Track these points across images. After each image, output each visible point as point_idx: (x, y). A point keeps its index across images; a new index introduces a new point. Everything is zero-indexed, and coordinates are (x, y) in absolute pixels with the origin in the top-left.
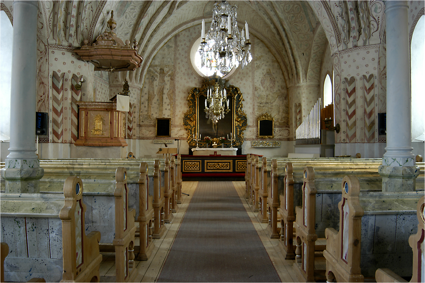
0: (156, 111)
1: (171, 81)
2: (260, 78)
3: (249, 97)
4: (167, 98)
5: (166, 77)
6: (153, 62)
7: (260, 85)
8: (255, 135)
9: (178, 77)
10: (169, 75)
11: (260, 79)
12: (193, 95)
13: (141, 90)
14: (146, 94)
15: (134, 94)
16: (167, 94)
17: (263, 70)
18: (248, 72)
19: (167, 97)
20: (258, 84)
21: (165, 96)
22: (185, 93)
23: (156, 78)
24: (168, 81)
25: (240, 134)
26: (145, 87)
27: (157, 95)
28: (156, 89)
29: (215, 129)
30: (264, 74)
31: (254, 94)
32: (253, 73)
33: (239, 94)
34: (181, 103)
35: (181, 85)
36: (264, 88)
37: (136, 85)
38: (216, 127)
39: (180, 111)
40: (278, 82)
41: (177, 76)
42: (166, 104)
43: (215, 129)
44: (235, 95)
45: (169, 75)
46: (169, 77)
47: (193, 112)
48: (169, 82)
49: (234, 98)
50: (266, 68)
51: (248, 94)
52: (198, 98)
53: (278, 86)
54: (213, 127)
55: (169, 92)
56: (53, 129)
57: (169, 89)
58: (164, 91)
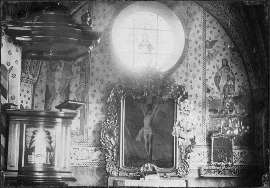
1: (82, 72)
2: (213, 73)
3: (198, 103)
5: (75, 66)
7: (213, 84)
8: (206, 160)
11: (213, 76)
12: (117, 97)
13: (35, 85)
14: (42, 91)
15: (28, 92)
16: (76, 92)
17: (218, 61)
18: (197, 63)
20: (210, 83)
22: (102, 92)
23: (58, 67)
24: (78, 72)
25: (186, 157)
26: (41, 81)
27: (59, 94)
28: (58, 85)
29: (148, 149)
30: (219, 68)
31: (204, 97)
32: (204, 65)
33: (184, 96)
34: (96, 108)
35: (97, 80)
36: (219, 89)
38: (150, 146)
40: (238, 80)
43: (148, 149)
44: (179, 97)
45: (79, 64)
46: (79, 67)
47: (115, 122)
48: (79, 75)
49: (177, 102)
50: (222, 57)
51: (196, 96)
52: (123, 100)
53: (239, 86)
54: (146, 146)
55: (78, 90)
57: (79, 85)
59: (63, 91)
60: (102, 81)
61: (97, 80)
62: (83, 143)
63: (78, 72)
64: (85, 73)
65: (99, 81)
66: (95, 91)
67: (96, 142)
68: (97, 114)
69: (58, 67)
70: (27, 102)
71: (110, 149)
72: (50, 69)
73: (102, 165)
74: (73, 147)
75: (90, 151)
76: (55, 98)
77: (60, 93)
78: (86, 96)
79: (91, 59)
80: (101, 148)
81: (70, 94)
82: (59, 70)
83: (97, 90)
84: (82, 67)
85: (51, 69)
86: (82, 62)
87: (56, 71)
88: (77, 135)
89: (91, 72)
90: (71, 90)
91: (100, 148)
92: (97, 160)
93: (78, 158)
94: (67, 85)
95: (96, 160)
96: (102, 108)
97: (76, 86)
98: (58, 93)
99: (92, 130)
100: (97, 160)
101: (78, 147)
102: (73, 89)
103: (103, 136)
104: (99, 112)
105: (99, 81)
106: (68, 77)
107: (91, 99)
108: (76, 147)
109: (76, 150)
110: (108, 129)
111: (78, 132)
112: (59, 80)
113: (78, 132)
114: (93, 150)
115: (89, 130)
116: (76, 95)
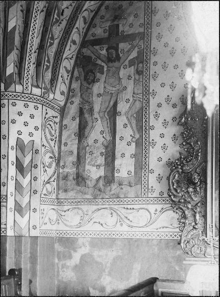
0: (99, 162)
4: (125, 126)
6: (90, 33)
9: (155, 63)
10: (132, 63)
15: (32, 116)
19: (127, 122)
21: (121, 121)
22: (174, 106)
23: (98, 75)
24: (129, 77)
37: (37, 91)
39: (160, 159)
41: (153, 59)
42: (124, 143)
45: (132, 63)
48: (132, 82)
56: (16, 156)
57: (131, 99)
58: (118, 105)
59: (106, 113)
60: (173, 86)
61: (163, 85)
62: (140, 199)
63: (129, 77)
64: (141, 76)
65: (167, 87)
66: (159, 105)
67: (163, 196)
68: (164, 147)
69: (98, 75)
70: (31, 134)
71: (188, 208)
72: (85, 80)
73: (175, 236)
74: (124, 206)
75: (153, 212)
76: (93, 127)
77: (102, 118)
78: (144, 117)
79: (152, 49)
80: (171, 206)
81: (117, 117)
82: (98, 80)
83: (164, 104)
84: (136, 68)
85: (86, 79)
86: (137, 58)
87: (94, 82)
88: (131, 186)
89: (152, 73)
90: (118, 109)
91: (170, 205)
92: (167, 227)
93: (132, 224)
94: (112, 103)
95: (163, 228)
96: (175, 135)
97: (128, 101)
98: (99, 118)
99: (156, 174)
100: (167, 227)
101: (132, 207)
102: (122, 107)
103: (173, 185)
104: (168, 140)
105: (167, 87)
106: (114, 89)
107: (153, 121)
108: (129, 207)
109: (129, 211)
110: (182, 172)
111: (132, 181)
112: (99, 95)
113: (132, 181)
114: (159, 209)
115: (150, 174)
116: (127, 118)
